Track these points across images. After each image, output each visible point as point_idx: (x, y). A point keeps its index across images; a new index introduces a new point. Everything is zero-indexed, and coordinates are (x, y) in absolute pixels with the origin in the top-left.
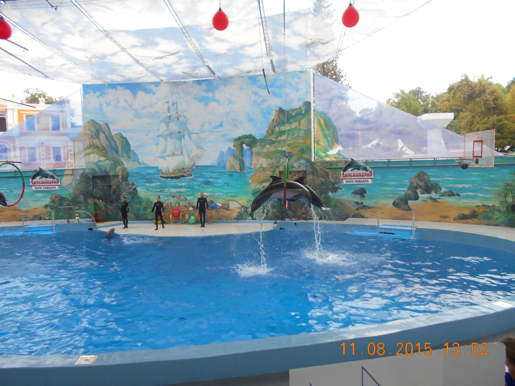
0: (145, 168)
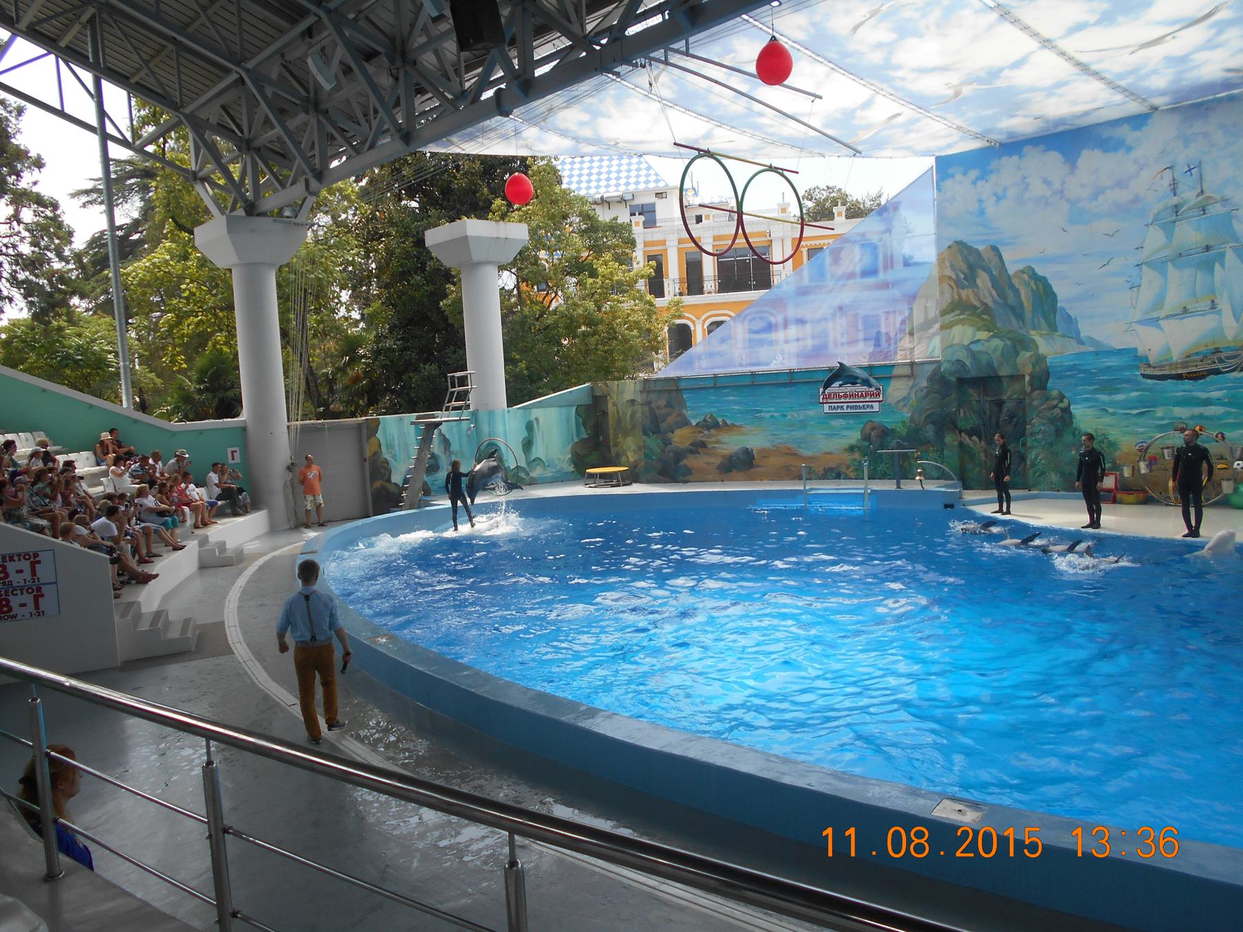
0: (1096, 353)
